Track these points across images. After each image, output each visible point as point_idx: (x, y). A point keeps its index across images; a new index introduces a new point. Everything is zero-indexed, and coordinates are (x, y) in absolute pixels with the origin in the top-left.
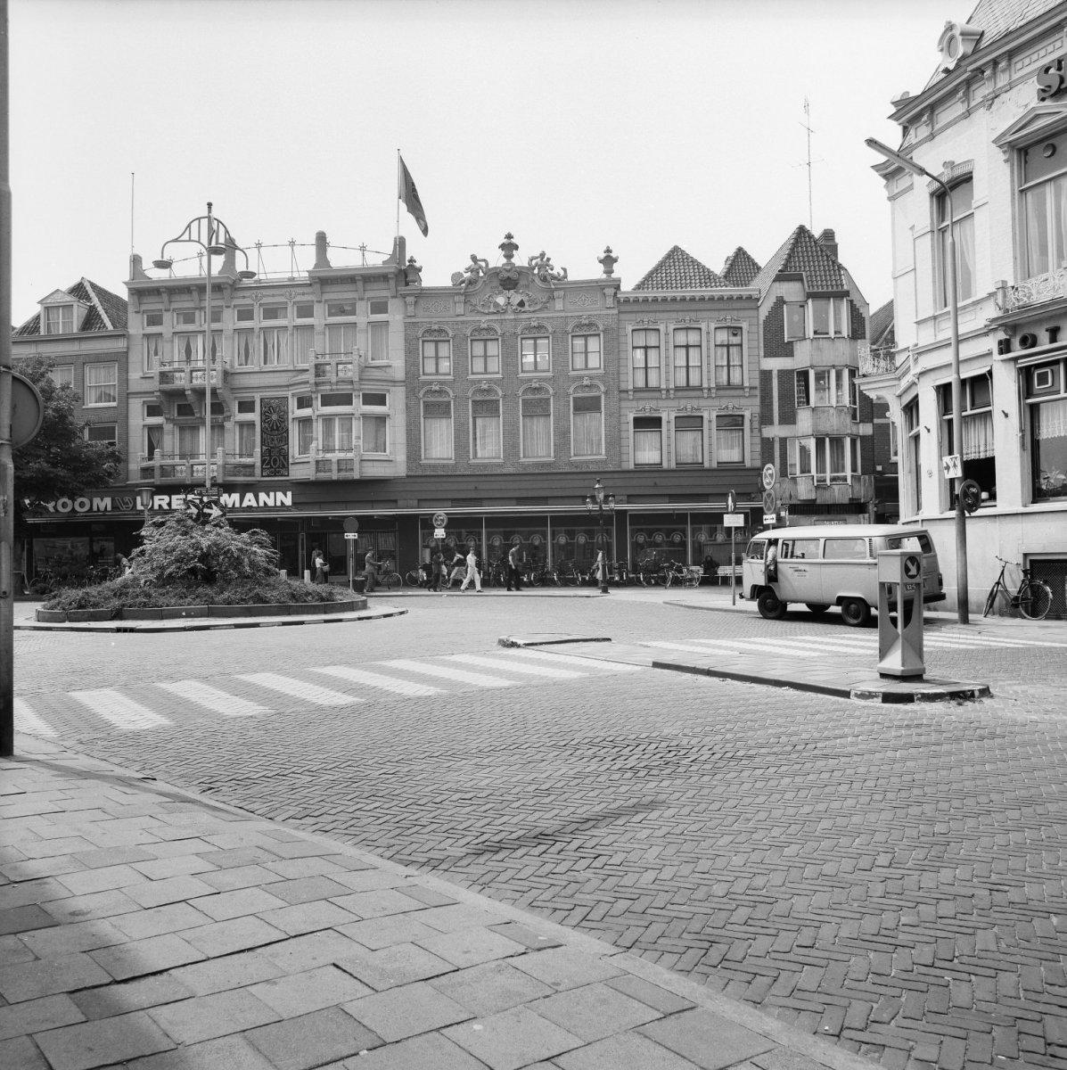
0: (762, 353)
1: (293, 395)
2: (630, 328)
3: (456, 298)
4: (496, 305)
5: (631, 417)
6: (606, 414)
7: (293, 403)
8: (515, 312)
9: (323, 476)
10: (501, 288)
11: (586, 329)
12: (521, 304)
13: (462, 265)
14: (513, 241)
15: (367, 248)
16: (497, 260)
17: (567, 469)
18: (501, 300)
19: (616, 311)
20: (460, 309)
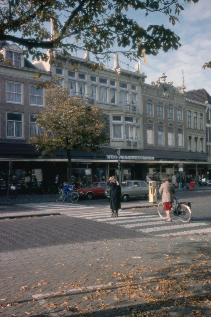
0: (206, 122)
1: (112, 115)
2: (187, 110)
3: (155, 90)
4: (163, 95)
5: (188, 136)
6: (184, 135)
7: (111, 118)
8: (167, 99)
9: (129, 148)
10: (164, 90)
11: (179, 108)
12: (168, 96)
13: (155, 81)
14: (166, 75)
15: (130, 65)
16: (162, 81)
17: (177, 150)
18: (164, 94)
19: (185, 104)
20: (156, 94)
